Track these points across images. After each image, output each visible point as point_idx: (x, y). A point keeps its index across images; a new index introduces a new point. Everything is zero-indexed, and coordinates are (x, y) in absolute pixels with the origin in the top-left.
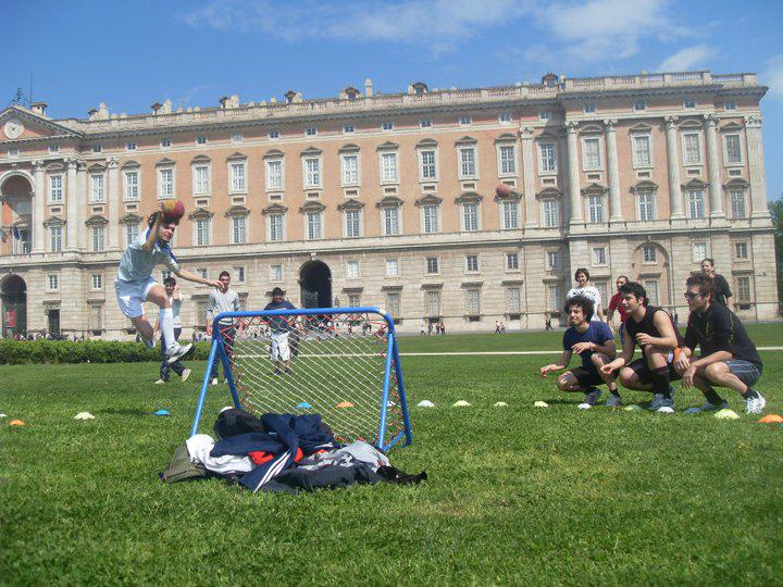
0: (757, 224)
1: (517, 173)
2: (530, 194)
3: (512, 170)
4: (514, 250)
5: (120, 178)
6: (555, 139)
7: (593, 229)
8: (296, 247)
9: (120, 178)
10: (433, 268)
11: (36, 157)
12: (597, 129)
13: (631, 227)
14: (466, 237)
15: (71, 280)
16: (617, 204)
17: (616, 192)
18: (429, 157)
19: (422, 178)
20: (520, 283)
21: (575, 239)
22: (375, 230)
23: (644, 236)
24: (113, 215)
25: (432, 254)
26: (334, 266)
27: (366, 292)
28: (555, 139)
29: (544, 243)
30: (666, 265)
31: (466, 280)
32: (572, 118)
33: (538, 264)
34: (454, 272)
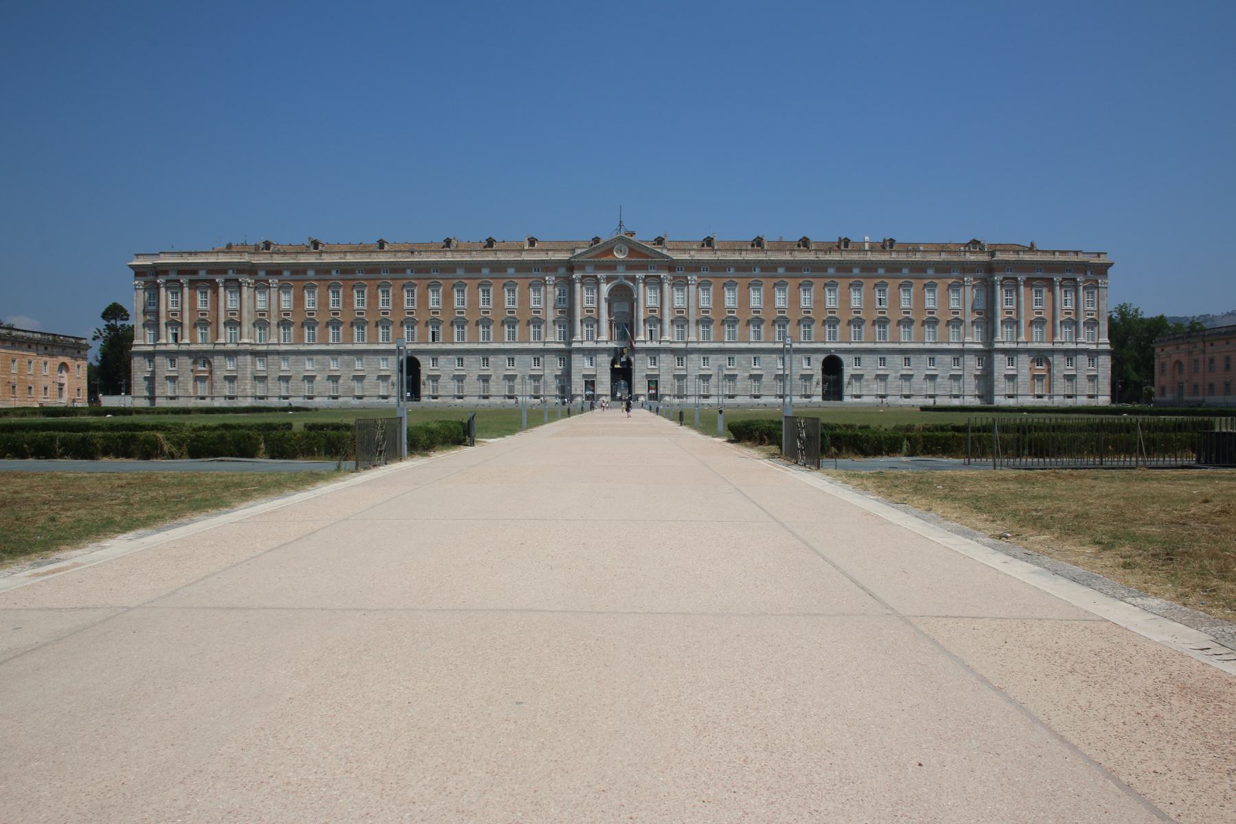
0: (1101, 347)
4: (959, 354)
5: (697, 292)
6: (989, 289)
9: (697, 292)
11: (639, 275)
15: (667, 361)
16: (1023, 330)
20: (960, 376)
23: (1039, 351)
24: (693, 318)
26: (847, 360)
28: (989, 289)
29: (975, 351)
30: (1049, 371)
32: (998, 278)
33: (972, 366)
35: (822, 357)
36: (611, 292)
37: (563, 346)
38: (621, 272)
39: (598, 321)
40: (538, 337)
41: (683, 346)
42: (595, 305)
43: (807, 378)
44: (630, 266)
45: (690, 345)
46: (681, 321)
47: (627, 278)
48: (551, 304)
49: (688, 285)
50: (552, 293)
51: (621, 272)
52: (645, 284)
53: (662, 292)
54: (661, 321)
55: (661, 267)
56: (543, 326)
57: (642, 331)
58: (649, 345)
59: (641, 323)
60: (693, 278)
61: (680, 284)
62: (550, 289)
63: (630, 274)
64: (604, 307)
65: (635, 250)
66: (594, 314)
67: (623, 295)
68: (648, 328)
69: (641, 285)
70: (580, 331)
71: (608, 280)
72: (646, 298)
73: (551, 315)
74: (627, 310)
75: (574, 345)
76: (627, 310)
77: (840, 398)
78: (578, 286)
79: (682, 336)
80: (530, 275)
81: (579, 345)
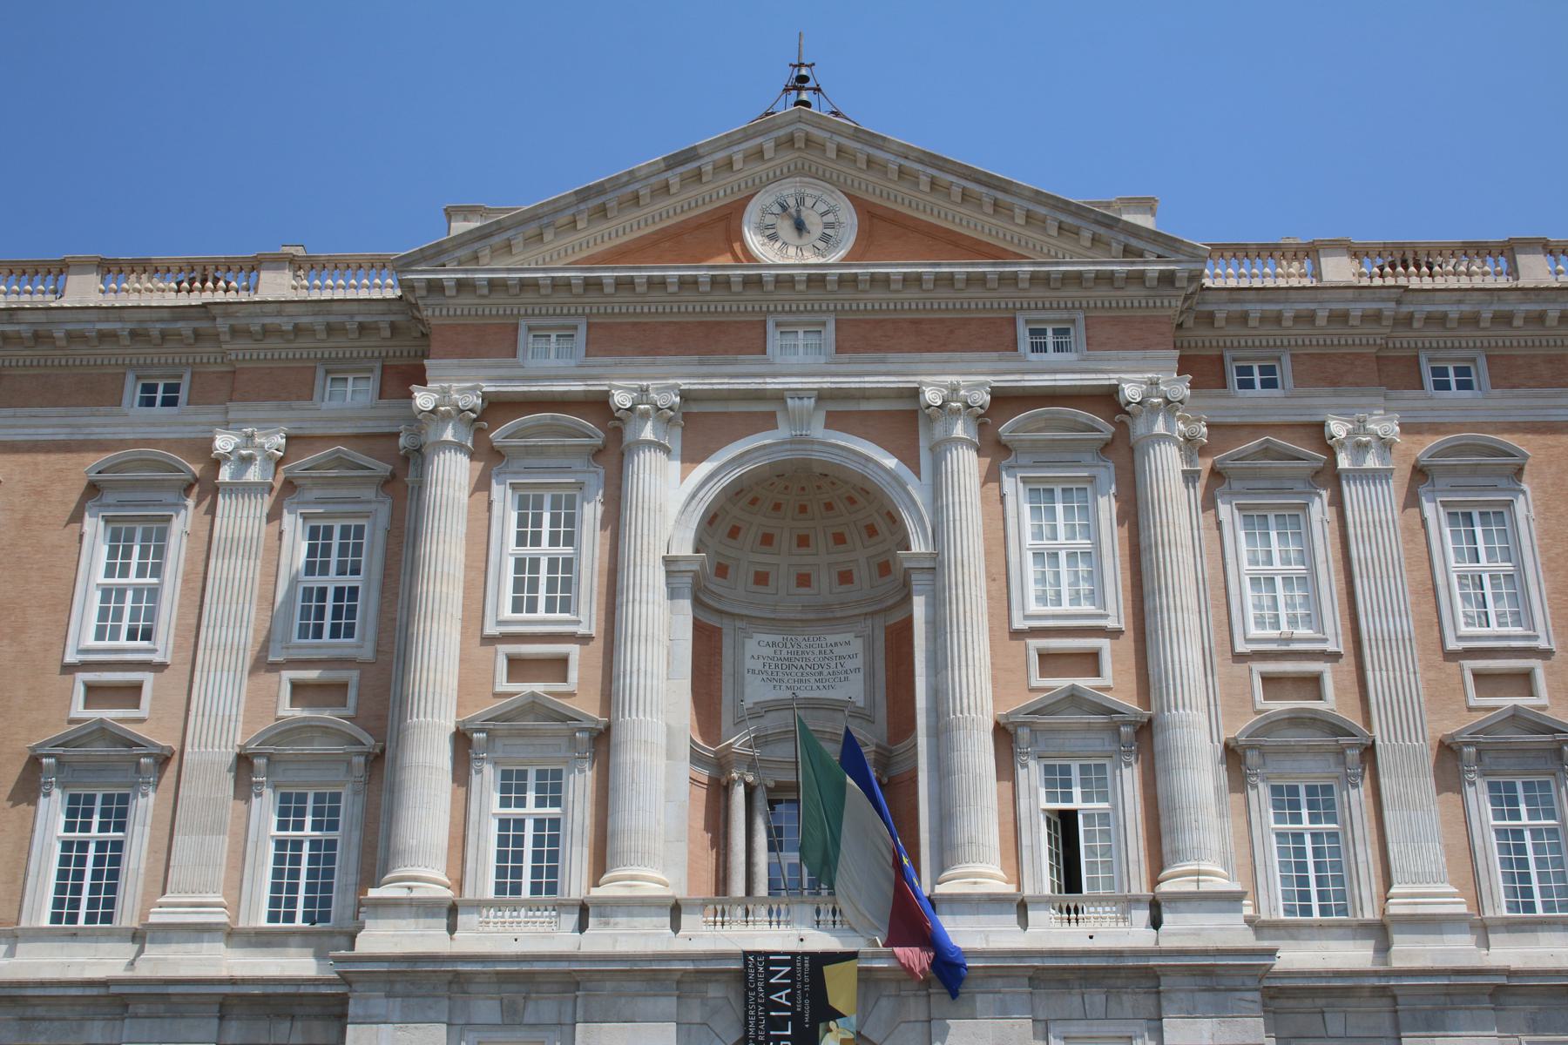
36: (720, 524)
37: (298, 965)
38: (798, 366)
39: (601, 743)
40: (90, 891)
41: (1355, 955)
42: (588, 618)
44: (867, 321)
45: (1411, 952)
46: (1307, 750)
47: (843, 409)
48: (235, 624)
49: (1331, 478)
50: (248, 555)
51: (798, 366)
52: (997, 452)
53: (1133, 513)
54: (1144, 737)
55: (1121, 332)
56: (145, 807)
57: (982, 819)
58: (1049, 932)
59: (977, 753)
60: (1370, 429)
61: (1273, 473)
62: (240, 518)
63: (878, 377)
64: (661, 634)
65: (904, 202)
66: (578, 691)
67: (813, 550)
68: (1037, 801)
69: (966, 465)
70: (433, 811)
71: (699, 426)
72: (1008, 565)
73: (223, 708)
74: (853, 690)
75: (381, 938)
76: (853, 690)
78: (451, 474)
79: (1320, 887)
80: (98, 424)
81: (427, 938)
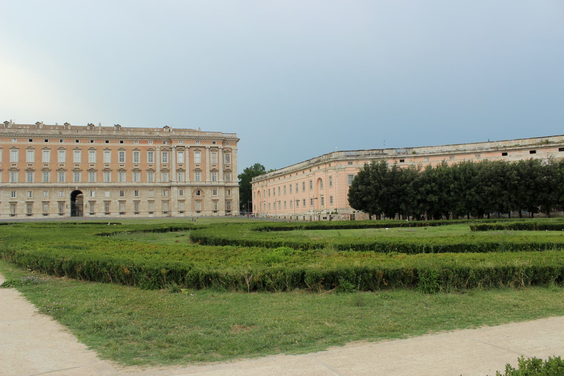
1: (153, 162)
2: (158, 170)
3: (152, 161)
7: (179, 184)
8: (70, 184)
10: (122, 194)
12: (180, 149)
13: (192, 184)
14: (134, 184)
17: (187, 171)
18: (122, 155)
19: (119, 162)
21: (173, 186)
22: (106, 180)
25: (122, 190)
27: (97, 203)
31: (134, 199)
34: (130, 198)
35: (70, 192)
43: (61, 203)
77: (82, 215)
